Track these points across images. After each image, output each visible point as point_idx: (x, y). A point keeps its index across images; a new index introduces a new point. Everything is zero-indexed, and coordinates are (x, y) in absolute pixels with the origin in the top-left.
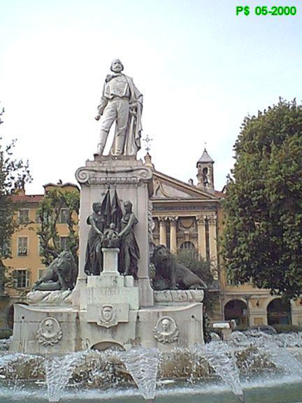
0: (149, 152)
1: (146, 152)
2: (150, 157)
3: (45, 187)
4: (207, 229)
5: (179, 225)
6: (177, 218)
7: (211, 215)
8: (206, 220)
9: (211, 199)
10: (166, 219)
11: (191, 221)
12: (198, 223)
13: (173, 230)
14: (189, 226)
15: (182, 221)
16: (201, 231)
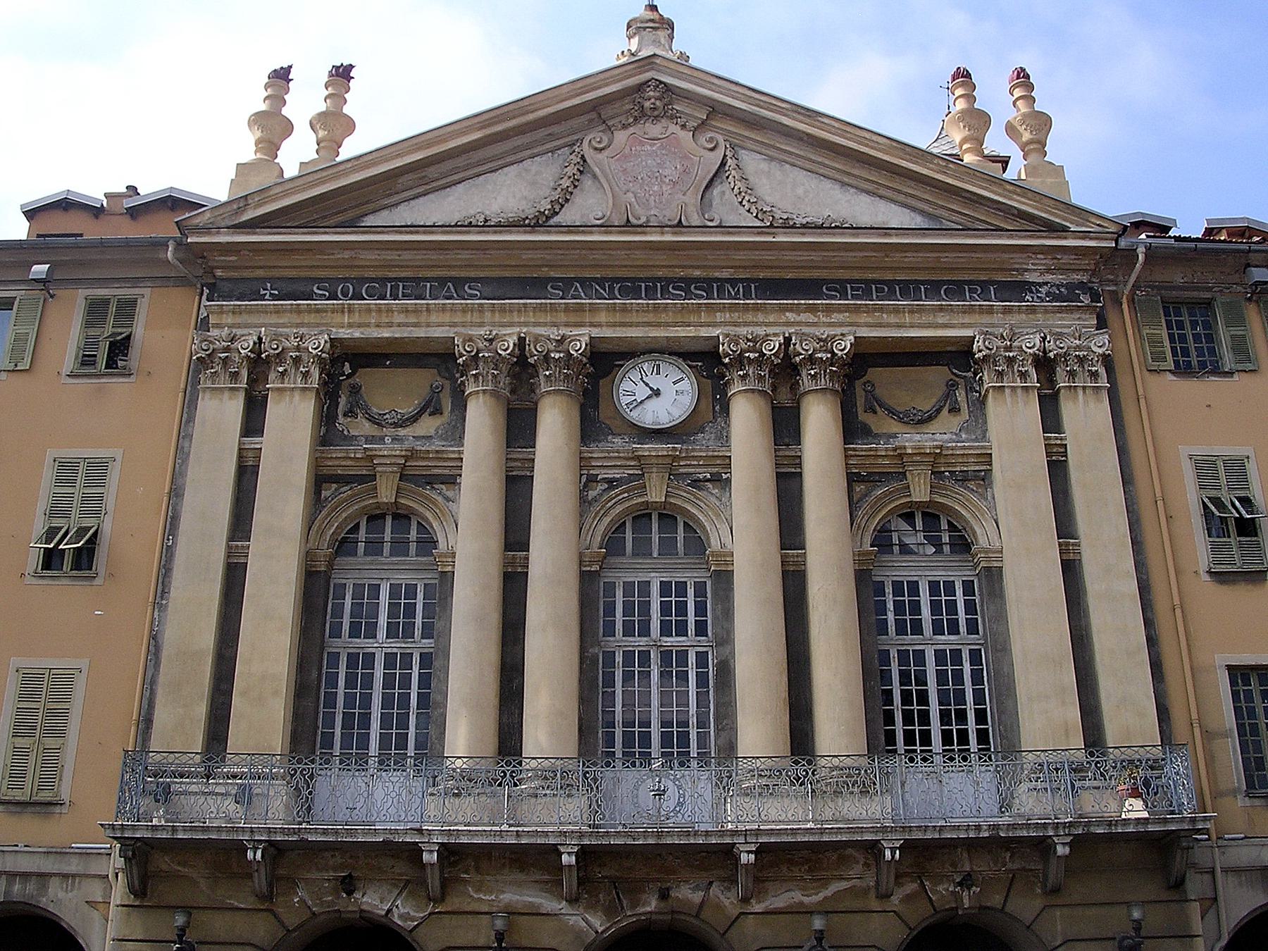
3: (31, 214)
4: (1051, 419)
5: (860, 402)
6: (847, 343)
8: (1045, 364)
9: (1060, 230)
10: (772, 347)
11: (937, 375)
13: (819, 421)
14: (926, 404)
15: (875, 374)
16: (1012, 422)
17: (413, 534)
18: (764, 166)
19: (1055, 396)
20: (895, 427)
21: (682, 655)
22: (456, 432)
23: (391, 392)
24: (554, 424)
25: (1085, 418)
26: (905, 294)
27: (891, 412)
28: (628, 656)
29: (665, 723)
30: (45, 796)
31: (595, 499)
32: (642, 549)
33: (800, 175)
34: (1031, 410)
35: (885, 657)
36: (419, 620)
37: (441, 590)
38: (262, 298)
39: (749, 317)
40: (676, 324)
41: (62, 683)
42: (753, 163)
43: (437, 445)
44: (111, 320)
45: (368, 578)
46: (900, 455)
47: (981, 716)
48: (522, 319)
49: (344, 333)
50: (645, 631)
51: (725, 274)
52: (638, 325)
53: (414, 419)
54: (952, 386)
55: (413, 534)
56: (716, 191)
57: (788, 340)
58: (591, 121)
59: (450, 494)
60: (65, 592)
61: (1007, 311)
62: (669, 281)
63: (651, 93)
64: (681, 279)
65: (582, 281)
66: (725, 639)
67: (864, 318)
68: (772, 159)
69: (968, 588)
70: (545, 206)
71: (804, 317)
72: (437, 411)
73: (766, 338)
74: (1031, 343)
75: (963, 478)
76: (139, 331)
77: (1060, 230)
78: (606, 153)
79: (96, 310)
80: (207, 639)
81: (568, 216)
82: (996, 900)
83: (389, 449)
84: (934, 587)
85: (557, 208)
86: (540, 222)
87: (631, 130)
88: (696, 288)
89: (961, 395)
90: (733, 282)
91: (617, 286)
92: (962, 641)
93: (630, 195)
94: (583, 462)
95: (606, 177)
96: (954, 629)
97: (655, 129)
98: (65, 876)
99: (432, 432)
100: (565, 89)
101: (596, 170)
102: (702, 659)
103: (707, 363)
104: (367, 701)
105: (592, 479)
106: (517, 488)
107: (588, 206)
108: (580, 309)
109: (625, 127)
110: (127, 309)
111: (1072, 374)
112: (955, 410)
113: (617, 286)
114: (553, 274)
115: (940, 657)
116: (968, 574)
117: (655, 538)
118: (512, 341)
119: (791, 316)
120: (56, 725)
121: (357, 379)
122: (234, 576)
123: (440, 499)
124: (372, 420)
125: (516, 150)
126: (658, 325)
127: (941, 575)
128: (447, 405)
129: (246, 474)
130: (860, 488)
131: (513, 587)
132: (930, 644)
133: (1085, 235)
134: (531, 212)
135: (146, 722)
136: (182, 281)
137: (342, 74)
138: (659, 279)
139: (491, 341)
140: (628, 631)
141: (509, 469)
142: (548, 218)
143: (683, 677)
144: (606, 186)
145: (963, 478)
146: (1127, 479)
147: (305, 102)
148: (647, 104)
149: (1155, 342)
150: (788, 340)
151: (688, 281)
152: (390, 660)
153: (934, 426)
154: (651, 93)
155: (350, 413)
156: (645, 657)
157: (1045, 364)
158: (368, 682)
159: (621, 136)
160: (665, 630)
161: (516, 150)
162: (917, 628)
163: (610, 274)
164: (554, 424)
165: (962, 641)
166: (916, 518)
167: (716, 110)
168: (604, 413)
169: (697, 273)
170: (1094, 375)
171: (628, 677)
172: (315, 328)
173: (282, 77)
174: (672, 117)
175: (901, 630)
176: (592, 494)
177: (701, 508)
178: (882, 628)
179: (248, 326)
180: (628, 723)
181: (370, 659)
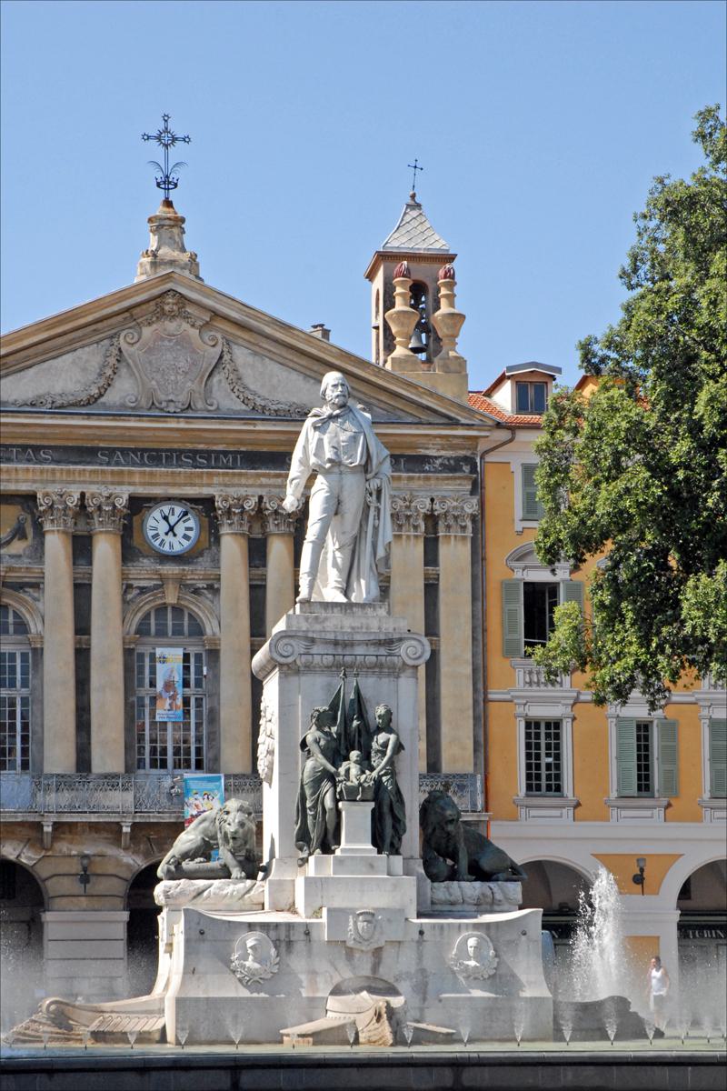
0: (173, 195)
1: (161, 194)
10: (250, 505)
17: (11, 619)
18: (250, 359)
22: (38, 551)
24: (105, 550)
31: (132, 600)
32: (161, 633)
33: (275, 368)
39: (236, 480)
40: (185, 485)
42: (241, 355)
43: (25, 563)
48: (82, 479)
51: (220, 448)
52: (160, 484)
53: (8, 543)
55: (11, 619)
56: (215, 379)
57: (261, 498)
58: (125, 319)
59: (36, 595)
62: (181, 452)
63: (170, 300)
64: (190, 451)
65: (123, 451)
66: (215, 695)
68: (255, 353)
70: (95, 391)
71: (272, 481)
72: (23, 537)
73: (246, 498)
78: (137, 345)
81: (112, 397)
85: (102, 391)
86: (91, 401)
87: (155, 326)
88: (200, 458)
90: (225, 453)
91: (146, 455)
93: (154, 383)
94: (124, 576)
95: (136, 366)
97: (171, 326)
99: (21, 552)
100: (107, 300)
101: (130, 361)
105: (129, 587)
106: (82, 591)
107: (123, 390)
108: (122, 472)
109: (149, 324)
113: (146, 455)
114: (101, 445)
117: (170, 623)
118: (76, 496)
119: (264, 480)
123: (29, 599)
125: (72, 342)
126: (174, 485)
128: (30, 531)
134: (84, 397)
138: (175, 451)
139: (61, 496)
141: (75, 579)
142: (96, 399)
144: (137, 374)
148: (167, 308)
150: (261, 498)
151: (195, 452)
154: (170, 300)
159: (147, 332)
161: (72, 342)
163: (141, 445)
164: (105, 550)
168: (136, 541)
169: (201, 447)
174: (184, 318)
176: (129, 597)
177: (200, 608)
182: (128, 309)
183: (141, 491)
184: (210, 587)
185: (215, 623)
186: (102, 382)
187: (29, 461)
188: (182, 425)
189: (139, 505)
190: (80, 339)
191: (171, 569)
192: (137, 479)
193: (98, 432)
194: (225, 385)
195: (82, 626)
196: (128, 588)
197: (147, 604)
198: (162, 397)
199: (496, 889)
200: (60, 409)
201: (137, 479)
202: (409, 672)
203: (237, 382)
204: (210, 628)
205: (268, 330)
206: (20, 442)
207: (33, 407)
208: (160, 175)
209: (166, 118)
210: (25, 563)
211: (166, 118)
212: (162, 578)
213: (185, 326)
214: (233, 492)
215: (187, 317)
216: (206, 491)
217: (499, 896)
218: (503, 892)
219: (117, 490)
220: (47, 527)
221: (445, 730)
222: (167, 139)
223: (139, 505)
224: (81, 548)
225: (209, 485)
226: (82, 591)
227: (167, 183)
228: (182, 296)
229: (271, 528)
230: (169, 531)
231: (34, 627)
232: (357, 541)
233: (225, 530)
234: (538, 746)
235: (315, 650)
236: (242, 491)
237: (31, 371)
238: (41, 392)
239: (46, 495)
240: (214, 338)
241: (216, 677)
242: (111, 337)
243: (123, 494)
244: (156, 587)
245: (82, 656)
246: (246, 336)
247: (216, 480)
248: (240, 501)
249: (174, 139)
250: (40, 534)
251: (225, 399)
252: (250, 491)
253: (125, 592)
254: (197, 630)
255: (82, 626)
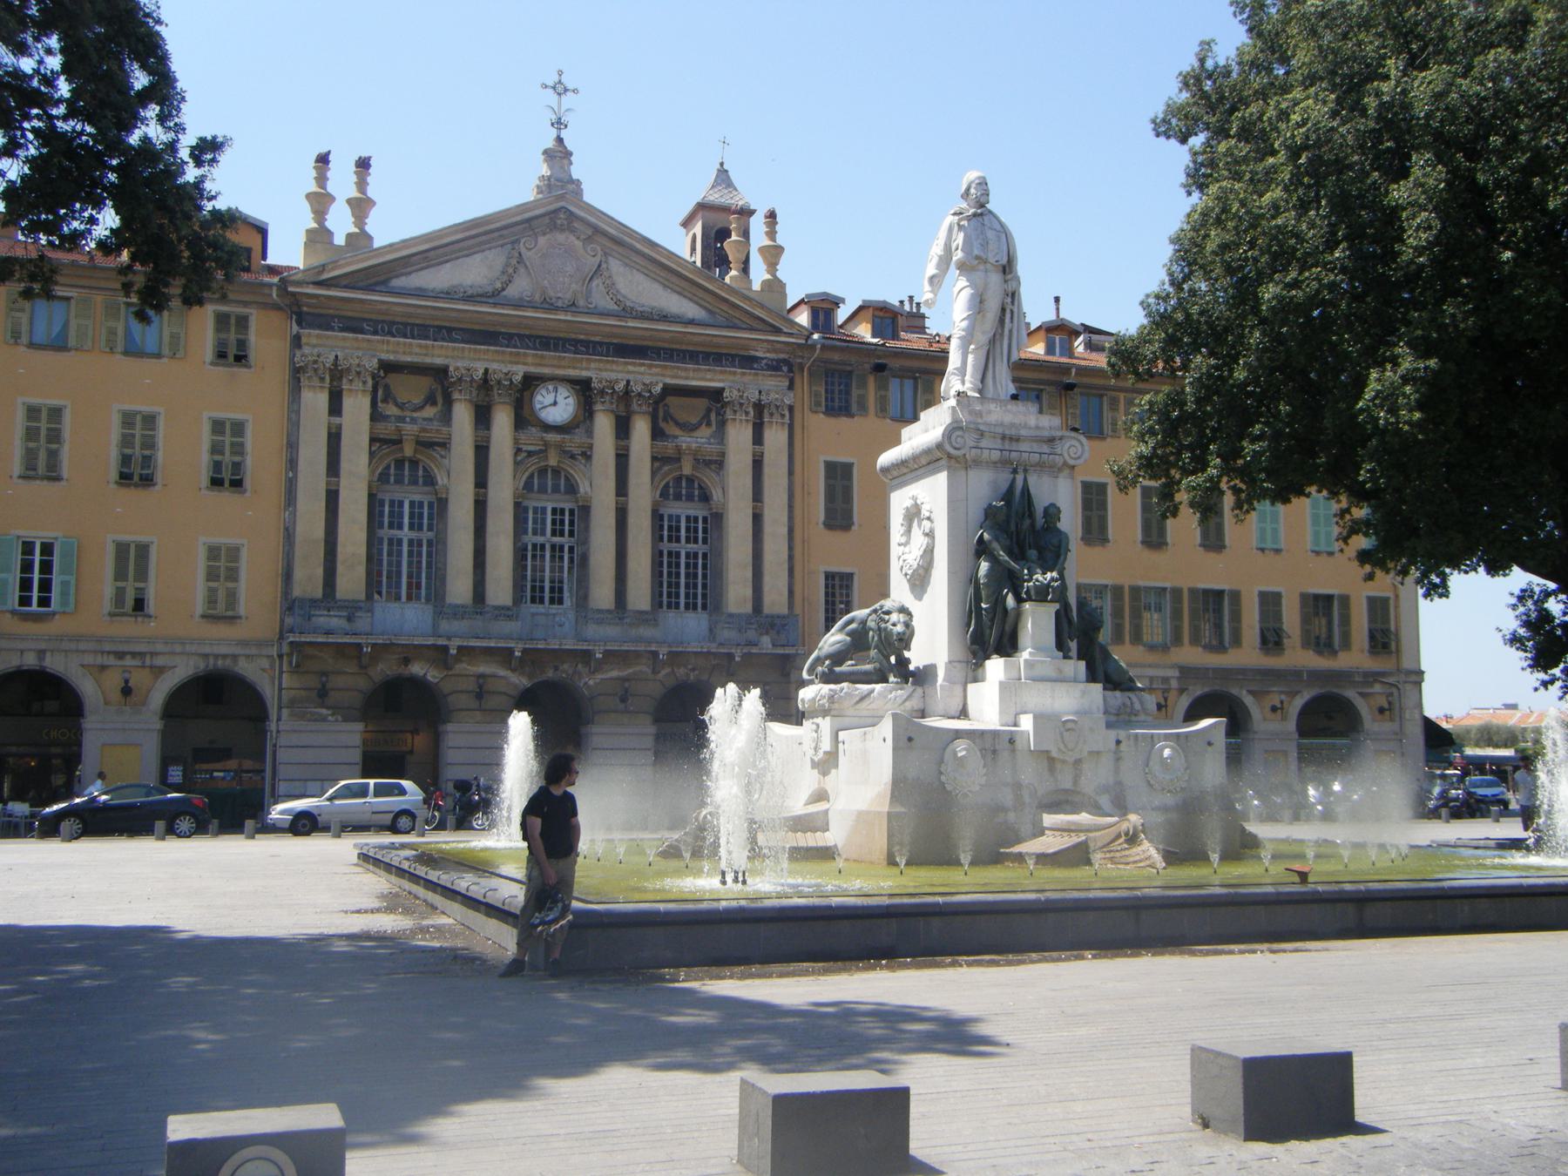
0: (564, 134)
1: (553, 133)
2: (569, 154)
4: (758, 439)
5: (661, 414)
6: (658, 389)
7: (771, 387)
8: (759, 408)
9: (778, 331)
10: (620, 386)
11: (702, 403)
12: (729, 415)
13: (641, 429)
14: (694, 421)
15: (670, 400)
16: (739, 436)
17: (421, 473)
19: (762, 424)
20: (678, 432)
21: (562, 548)
22: (446, 417)
23: (410, 390)
24: (502, 420)
25: (775, 437)
26: (691, 357)
27: (677, 424)
28: (534, 546)
29: (552, 581)
30: (230, 613)
33: (641, 277)
34: (747, 433)
35: (661, 553)
36: (425, 521)
37: (441, 506)
38: (332, 329)
41: (234, 553)
42: (615, 266)
44: (233, 329)
45: (397, 497)
46: (678, 449)
47: (704, 586)
49: (384, 356)
50: (543, 533)
51: (597, 339)
53: (422, 407)
54: (709, 410)
55: (421, 473)
56: (594, 283)
57: (628, 382)
60: (226, 497)
61: (744, 374)
62: (565, 340)
66: (585, 541)
67: (669, 372)
69: (705, 520)
70: (498, 285)
72: (434, 403)
73: (617, 381)
74: (753, 395)
75: (708, 463)
76: (252, 337)
77: (778, 331)
79: (222, 321)
80: (319, 532)
82: (705, 677)
83: (410, 429)
84: (688, 518)
86: (496, 293)
89: (713, 416)
90: (601, 344)
92: (699, 548)
94: (516, 441)
96: (696, 541)
97: (560, 237)
98: (247, 656)
102: (571, 549)
103: (583, 388)
104: (399, 564)
106: (482, 452)
107: (520, 287)
108: (518, 354)
110: (243, 322)
111: (771, 415)
112: (709, 424)
115: (688, 555)
116: (706, 513)
118: (481, 371)
119: (631, 368)
120: (233, 575)
121: (387, 380)
122: (332, 498)
124: (397, 405)
126: (559, 367)
127: (692, 513)
128: (440, 400)
129: (334, 438)
130: (657, 464)
131: (481, 506)
132: (684, 548)
133: (790, 335)
134: (490, 289)
135: (288, 576)
136: (276, 307)
137: (363, 164)
140: (535, 533)
143: (561, 558)
145: (708, 463)
146: (791, 473)
147: (342, 182)
149: (817, 395)
152: (411, 542)
153: (698, 433)
155: (385, 401)
156: (543, 547)
157: (759, 408)
158: (400, 553)
159: (542, 240)
160: (554, 533)
162: (678, 540)
163: (534, 332)
164: (502, 420)
165: (699, 548)
166: (687, 483)
167: (597, 230)
168: (526, 412)
170: (783, 416)
171: (534, 556)
172: (364, 352)
173: (323, 160)
175: (670, 540)
177: (577, 472)
178: (661, 539)
179: (325, 346)
180: (534, 580)
181: (400, 542)
182: (528, 221)
183: (532, 369)
184: (584, 454)
185: (587, 483)
186: (505, 278)
187: (443, 340)
188: (569, 318)
189: (531, 382)
190: (488, 242)
191: (552, 437)
192: (530, 360)
193: (502, 319)
194: (601, 287)
195: (481, 481)
196: (518, 451)
197: (533, 465)
198: (552, 294)
199: (1135, 700)
200: (469, 298)
201: (530, 360)
202: (1066, 472)
203: (610, 288)
204: (583, 488)
205: (638, 246)
206: (437, 323)
207: (448, 295)
208: (554, 117)
209: (560, 73)
210: (435, 425)
211: (560, 73)
212: (546, 444)
213: (572, 238)
214: (605, 375)
215: (573, 231)
216: (585, 374)
217: (1137, 706)
218: (1142, 703)
219: (515, 368)
220: (456, 396)
221: (767, 579)
222: (560, 89)
223: (531, 382)
224: (483, 417)
225: (587, 369)
226: (482, 452)
227: (559, 124)
228: (571, 213)
229: (635, 407)
230: (556, 406)
231: (441, 480)
232: (993, 341)
233: (598, 407)
234: (834, 595)
235: (984, 444)
236: (613, 376)
237: (448, 265)
238: (455, 282)
239: (457, 369)
240: (594, 250)
241: (587, 529)
242: (513, 243)
243: (519, 372)
244: (541, 451)
245: (481, 506)
246: (620, 250)
247: (593, 365)
248: (612, 384)
249: (566, 90)
250: (449, 402)
251: (602, 301)
252: (620, 376)
253: (516, 454)
254: (572, 489)
255: (481, 481)
